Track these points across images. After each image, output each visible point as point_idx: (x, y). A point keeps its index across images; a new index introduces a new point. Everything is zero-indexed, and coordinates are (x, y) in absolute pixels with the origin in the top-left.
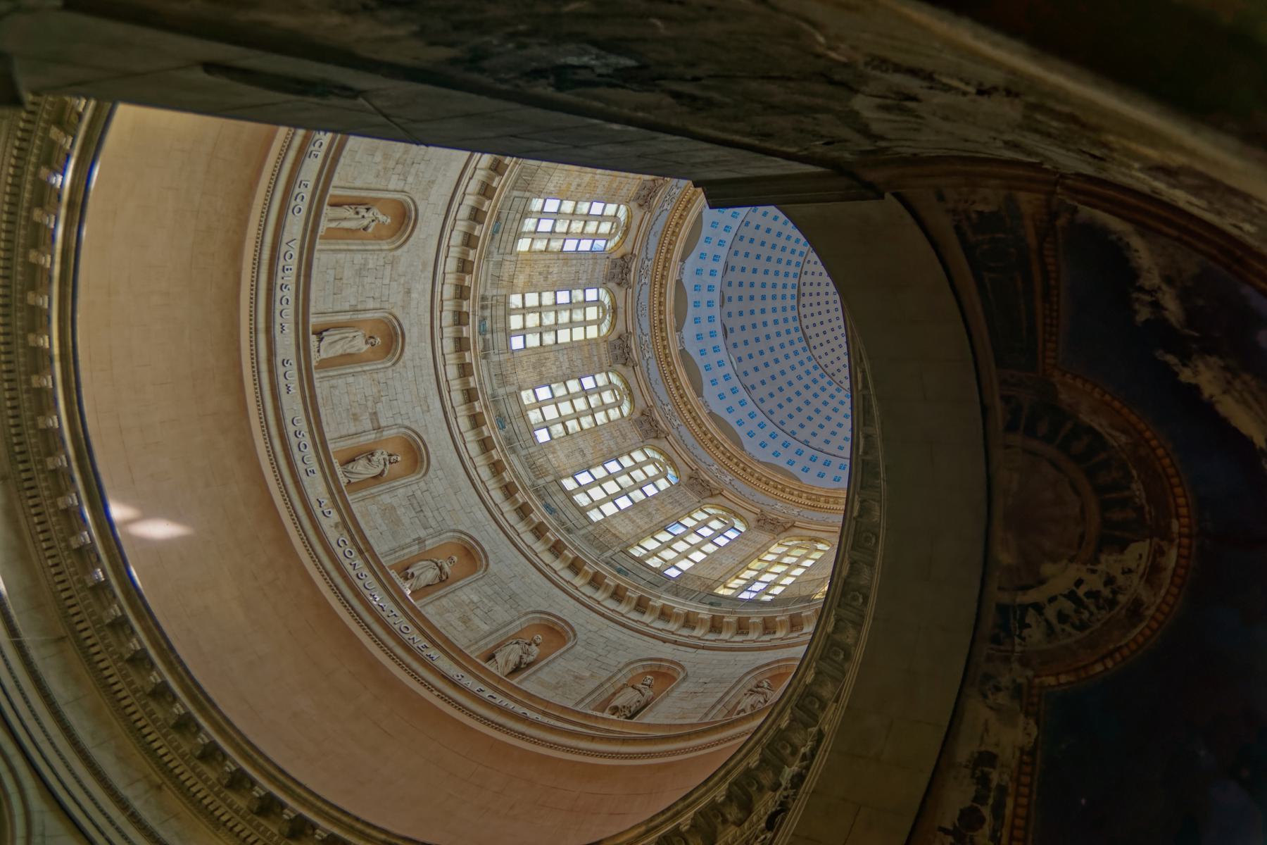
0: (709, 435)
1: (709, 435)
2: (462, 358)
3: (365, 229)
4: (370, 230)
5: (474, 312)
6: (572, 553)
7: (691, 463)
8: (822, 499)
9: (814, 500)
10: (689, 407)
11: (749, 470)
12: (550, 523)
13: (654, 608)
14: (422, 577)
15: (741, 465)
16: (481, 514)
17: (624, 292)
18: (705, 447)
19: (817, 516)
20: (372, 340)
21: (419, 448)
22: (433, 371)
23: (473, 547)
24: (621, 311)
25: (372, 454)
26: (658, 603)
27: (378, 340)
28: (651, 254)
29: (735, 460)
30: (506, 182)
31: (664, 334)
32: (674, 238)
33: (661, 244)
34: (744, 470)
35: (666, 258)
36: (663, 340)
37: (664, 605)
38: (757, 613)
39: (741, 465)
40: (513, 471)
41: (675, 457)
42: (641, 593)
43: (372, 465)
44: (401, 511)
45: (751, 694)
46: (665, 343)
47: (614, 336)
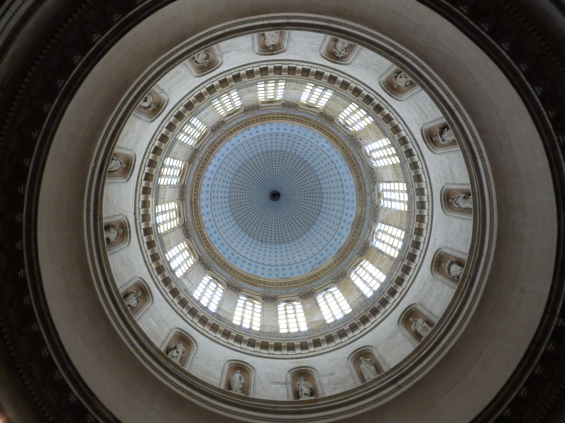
0: (214, 148)
1: (214, 148)
2: (257, 73)
3: (335, 47)
4: (334, 50)
5: (282, 77)
6: (163, 148)
7: (202, 146)
8: (196, 206)
9: (194, 202)
10: (227, 137)
11: (202, 170)
12: (176, 131)
13: (147, 198)
14: (145, 103)
15: (203, 166)
16: (176, 101)
17: (279, 105)
18: (209, 148)
19: (188, 207)
20: (271, 46)
21: (210, 69)
22: (250, 62)
23: (160, 108)
24: (271, 104)
25: (208, 59)
26: (150, 199)
27: (271, 49)
28: (296, 113)
29: (205, 162)
30: (348, 95)
31: (259, 121)
32: (304, 122)
33: (302, 117)
34: (202, 167)
35: (295, 119)
36: (256, 120)
37: (150, 201)
38: (159, 248)
39: (203, 166)
40: (200, 105)
41: (204, 139)
42: (152, 188)
43: (203, 60)
44: (178, 77)
45: (136, 299)
46: (255, 122)
47: (258, 104)
